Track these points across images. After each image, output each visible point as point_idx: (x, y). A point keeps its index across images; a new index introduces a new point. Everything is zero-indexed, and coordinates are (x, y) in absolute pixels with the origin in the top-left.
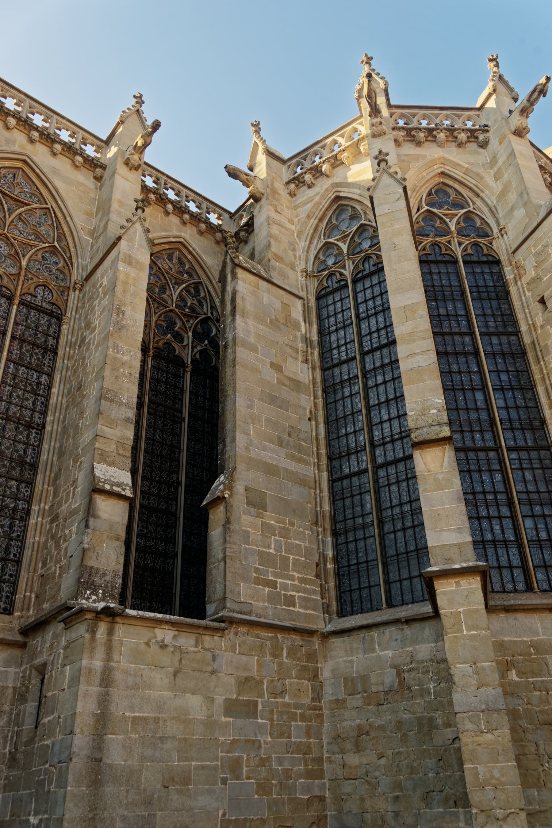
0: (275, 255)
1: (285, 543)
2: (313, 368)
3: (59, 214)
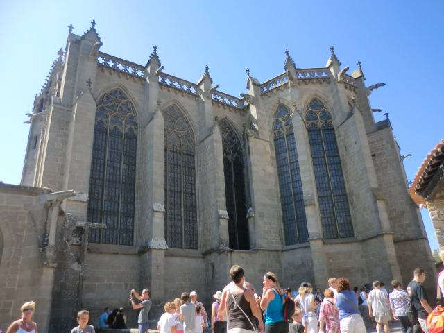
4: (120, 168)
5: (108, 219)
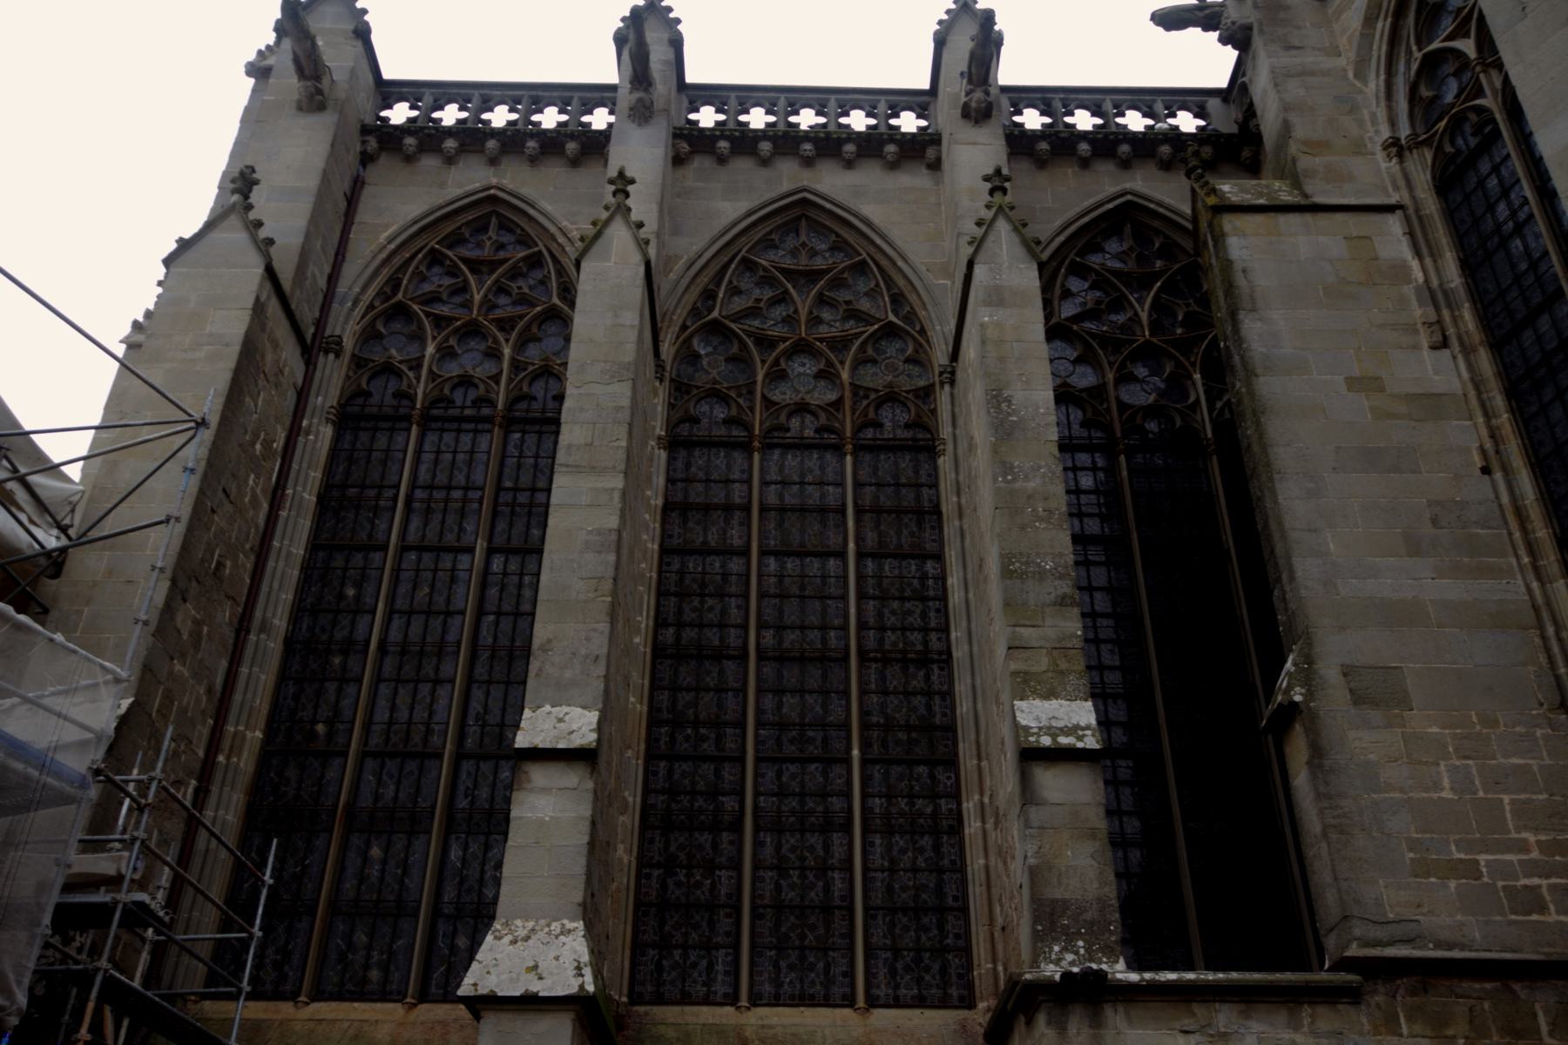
0: (1307, 143)
2: (1468, 351)
5: (376, 852)
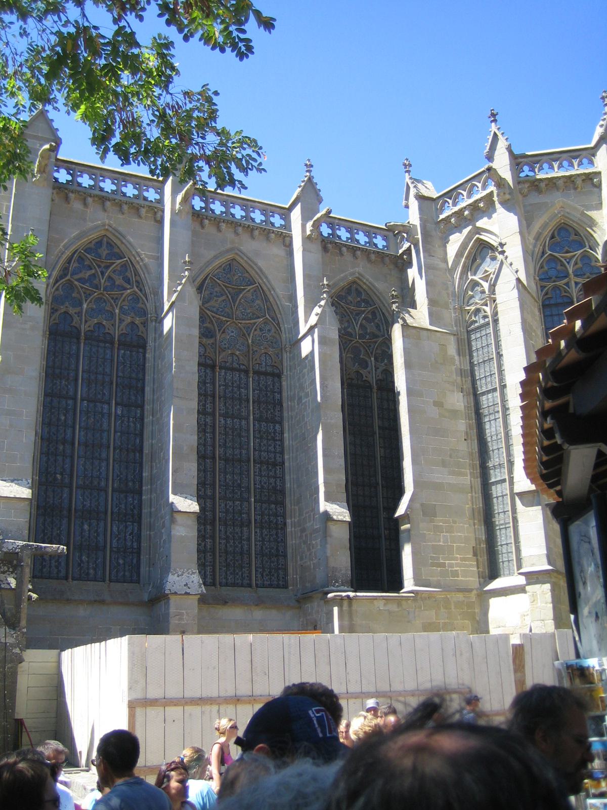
1: (450, 536)
3: (265, 288)
4: (110, 415)
5: (86, 527)
